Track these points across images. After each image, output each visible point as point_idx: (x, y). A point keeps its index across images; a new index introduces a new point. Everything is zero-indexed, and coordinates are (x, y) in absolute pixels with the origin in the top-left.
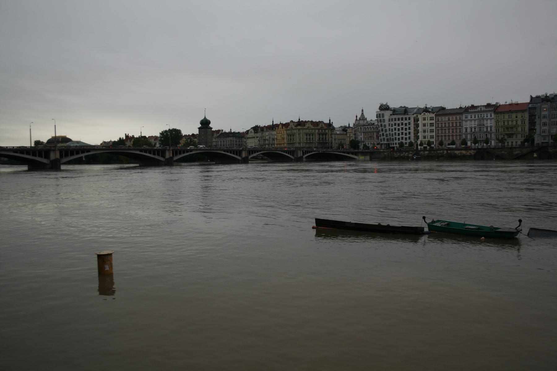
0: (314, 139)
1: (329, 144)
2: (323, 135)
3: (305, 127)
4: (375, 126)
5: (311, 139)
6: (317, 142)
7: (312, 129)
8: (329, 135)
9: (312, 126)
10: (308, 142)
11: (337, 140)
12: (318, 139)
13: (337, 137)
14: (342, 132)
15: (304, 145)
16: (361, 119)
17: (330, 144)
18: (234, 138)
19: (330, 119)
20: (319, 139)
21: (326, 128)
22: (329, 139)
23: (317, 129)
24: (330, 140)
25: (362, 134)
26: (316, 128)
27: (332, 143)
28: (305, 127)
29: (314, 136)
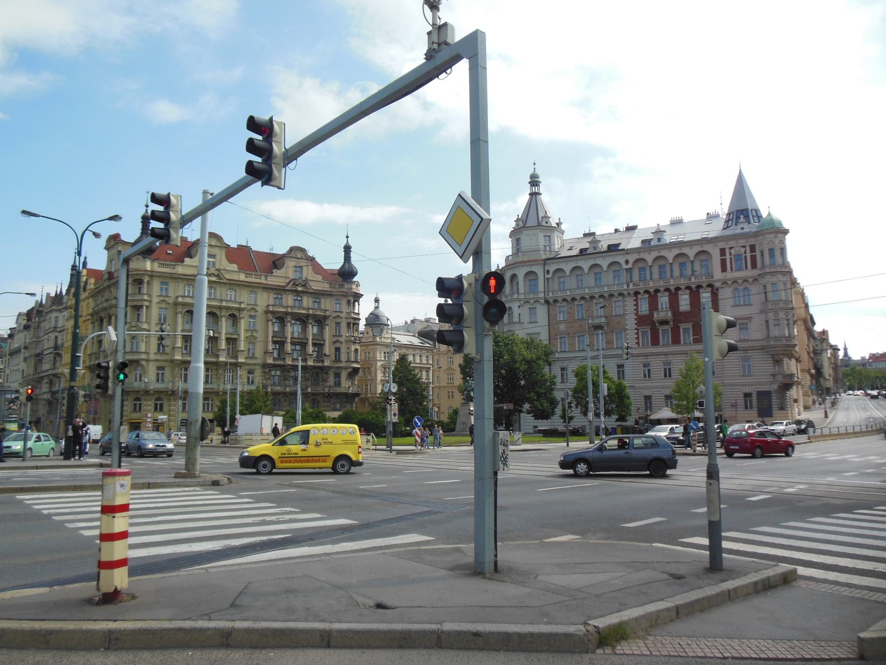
1: (338, 376)
2: (303, 320)
3: (180, 270)
4: (632, 258)
5: (223, 345)
7: (233, 284)
8: (338, 324)
9: (234, 267)
12: (271, 346)
14: (416, 341)
16: (532, 222)
17: (344, 375)
19: (351, 243)
20: (280, 343)
21: (326, 287)
22: (338, 350)
23: (267, 288)
24: (343, 357)
25: (542, 312)
28: (180, 270)
29: (243, 324)
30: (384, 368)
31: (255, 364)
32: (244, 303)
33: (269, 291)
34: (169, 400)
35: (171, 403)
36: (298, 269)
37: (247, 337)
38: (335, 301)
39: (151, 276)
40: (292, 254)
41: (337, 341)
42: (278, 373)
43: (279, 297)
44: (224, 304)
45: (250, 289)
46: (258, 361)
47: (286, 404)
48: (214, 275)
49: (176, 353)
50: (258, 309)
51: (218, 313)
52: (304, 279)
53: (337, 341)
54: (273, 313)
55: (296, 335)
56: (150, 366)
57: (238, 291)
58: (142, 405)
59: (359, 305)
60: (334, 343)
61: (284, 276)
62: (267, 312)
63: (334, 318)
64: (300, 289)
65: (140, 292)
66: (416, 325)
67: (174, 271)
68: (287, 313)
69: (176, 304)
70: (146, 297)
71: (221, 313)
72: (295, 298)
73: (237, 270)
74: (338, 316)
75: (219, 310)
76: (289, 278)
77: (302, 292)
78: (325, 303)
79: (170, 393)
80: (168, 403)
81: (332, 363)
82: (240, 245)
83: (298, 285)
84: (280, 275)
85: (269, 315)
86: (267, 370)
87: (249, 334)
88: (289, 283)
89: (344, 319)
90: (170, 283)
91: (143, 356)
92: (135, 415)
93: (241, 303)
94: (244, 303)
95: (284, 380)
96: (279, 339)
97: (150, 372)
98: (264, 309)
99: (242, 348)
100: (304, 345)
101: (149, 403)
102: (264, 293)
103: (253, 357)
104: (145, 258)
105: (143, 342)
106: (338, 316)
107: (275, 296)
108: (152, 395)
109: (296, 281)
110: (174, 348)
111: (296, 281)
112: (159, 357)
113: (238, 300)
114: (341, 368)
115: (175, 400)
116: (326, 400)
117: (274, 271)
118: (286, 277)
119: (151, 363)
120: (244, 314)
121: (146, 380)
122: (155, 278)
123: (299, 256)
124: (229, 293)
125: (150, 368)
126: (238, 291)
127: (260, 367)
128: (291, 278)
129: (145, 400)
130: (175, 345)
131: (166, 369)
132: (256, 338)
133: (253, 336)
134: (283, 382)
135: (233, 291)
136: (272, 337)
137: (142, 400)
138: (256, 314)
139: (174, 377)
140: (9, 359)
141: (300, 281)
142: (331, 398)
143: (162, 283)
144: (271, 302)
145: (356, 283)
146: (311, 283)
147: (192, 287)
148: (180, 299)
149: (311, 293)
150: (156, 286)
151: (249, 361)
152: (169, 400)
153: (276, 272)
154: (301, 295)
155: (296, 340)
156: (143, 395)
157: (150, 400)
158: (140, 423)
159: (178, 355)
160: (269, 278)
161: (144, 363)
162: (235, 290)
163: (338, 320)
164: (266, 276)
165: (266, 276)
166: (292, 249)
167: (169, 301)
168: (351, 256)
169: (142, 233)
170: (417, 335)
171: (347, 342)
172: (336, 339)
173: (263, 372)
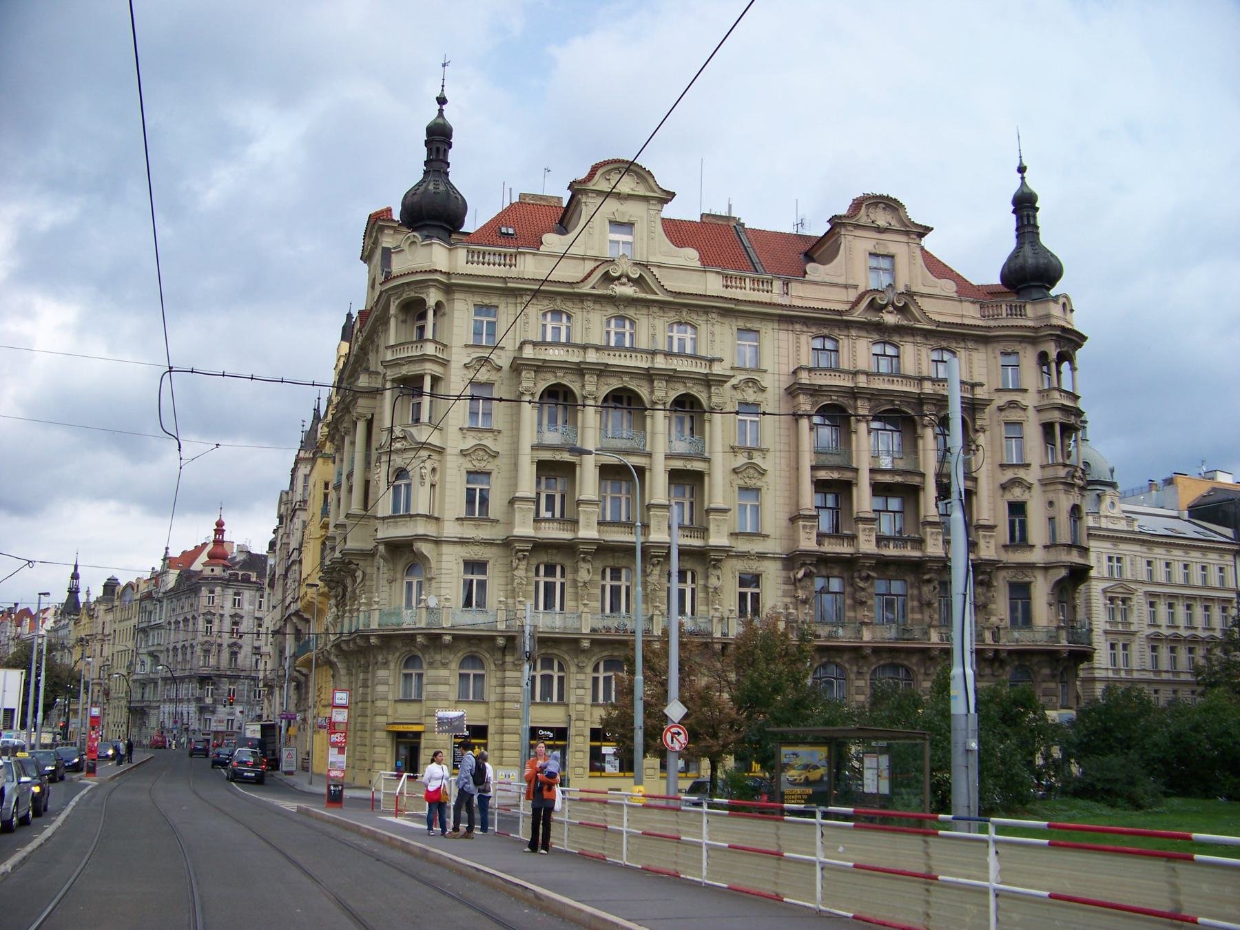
0: (719, 491)
1: (1021, 591)
3: (529, 267)
6: (792, 560)
9: (690, 256)
10: (588, 531)
11: (1139, 605)
12: (809, 499)
13: (1135, 562)
14: (1189, 530)
15: (495, 593)
17: (1041, 591)
18: (247, 595)
19: (1033, 185)
21: (970, 314)
22: (1017, 509)
23: (789, 319)
24: (1037, 532)
26: (775, 294)
27: (1079, 574)
28: (529, 267)
29: (720, 430)
30: (1112, 600)
31: (761, 556)
32: (721, 360)
33: (798, 327)
34: (502, 667)
35: (508, 674)
36: (884, 263)
37: (735, 471)
38: (1001, 360)
39: (449, 289)
40: (863, 218)
41: (1016, 482)
42: (835, 585)
43: (829, 345)
44: (660, 362)
45: (741, 324)
46: (773, 546)
47: (861, 683)
48: (630, 279)
49: (518, 517)
50: (766, 381)
51: (644, 392)
52: (901, 289)
53: (1016, 482)
54: (814, 391)
55: (886, 462)
56: (445, 558)
57: (703, 328)
58: (425, 680)
59: (1073, 369)
60: (1004, 487)
61: (842, 281)
62: (793, 391)
63: (1001, 409)
64: (890, 319)
65: (421, 339)
66: (1180, 488)
67: (514, 272)
68: (854, 394)
69: (518, 367)
70: (430, 349)
71: (652, 392)
72: (878, 349)
73: (698, 264)
74: (1013, 405)
75: (645, 384)
76: (856, 287)
77: (898, 330)
78: (970, 362)
79: (501, 642)
80: (499, 674)
81: (1002, 551)
82: (708, 215)
83: (885, 306)
84: (827, 279)
85: (802, 398)
86: (800, 574)
87: (741, 460)
88: (855, 304)
89: (1031, 412)
90: (502, 308)
91: (421, 528)
92: (407, 712)
93: (711, 361)
94: (721, 360)
95: (853, 608)
96: (835, 475)
97: (444, 578)
98: (785, 382)
99: (718, 503)
100: (910, 492)
101: (443, 672)
102: (783, 335)
103: (758, 535)
104: (429, 237)
105: (422, 484)
106: (1013, 405)
107: (818, 344)
108: (448, 647)
109: (878, 296)
110: (512, 501)
111: (878, 296)
112: (469, 532)
113: (703, 353)
114: (1031, 566)
115: (517, 667)
116: (988, 671)
117: (810, 267)
118: (846, 287)
119: (446, 549)
120: (725, 396)
121: (432, 602)
122: (457, 296)
123: (881, 222)
124: (676, 336)
125: (444, 565)
126: (703, 328)
127: (779, 565)
128: (861, 289)
129: (431, 665)
130: (515, 491)
131: (489, 567)
132: (762, 473)
133: (754, 466)
134: (850, 614)
135: (689, 328)
136: (813, 468)
137: (425, 666)
138: (759, 397)
139: (513, 593)
140: (269, 594)
141: (890, 296)
142: (1002, 663)
143: (481, 309)
144: (807, 359)
145: (1061, 300)
146: (925, 304)
147: (564, 317)
148: (528, 352)
149: (927, 334)
150: (462, 315)
151: (742, 546)
152: (502, 667)
153: (815, 271)
154: (896, 339)
155: (887, 479)
156: (425, 648)
157: (445, 665)
158: (418, 735)
159: (523, 524)
160: (796, 289)
161: (425, 548)
162: (694, 327)
163: (1014, 416)
164: (786, 283)
165: (786, 283)
166: (857, 205)
167: (499, 362)
168: (1039, 222)
169: (426, 173)
170: (1186, 515)
171: (1045, 483)
172: (1009, 474)
173: (787, 581)
